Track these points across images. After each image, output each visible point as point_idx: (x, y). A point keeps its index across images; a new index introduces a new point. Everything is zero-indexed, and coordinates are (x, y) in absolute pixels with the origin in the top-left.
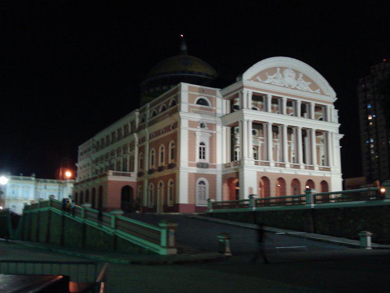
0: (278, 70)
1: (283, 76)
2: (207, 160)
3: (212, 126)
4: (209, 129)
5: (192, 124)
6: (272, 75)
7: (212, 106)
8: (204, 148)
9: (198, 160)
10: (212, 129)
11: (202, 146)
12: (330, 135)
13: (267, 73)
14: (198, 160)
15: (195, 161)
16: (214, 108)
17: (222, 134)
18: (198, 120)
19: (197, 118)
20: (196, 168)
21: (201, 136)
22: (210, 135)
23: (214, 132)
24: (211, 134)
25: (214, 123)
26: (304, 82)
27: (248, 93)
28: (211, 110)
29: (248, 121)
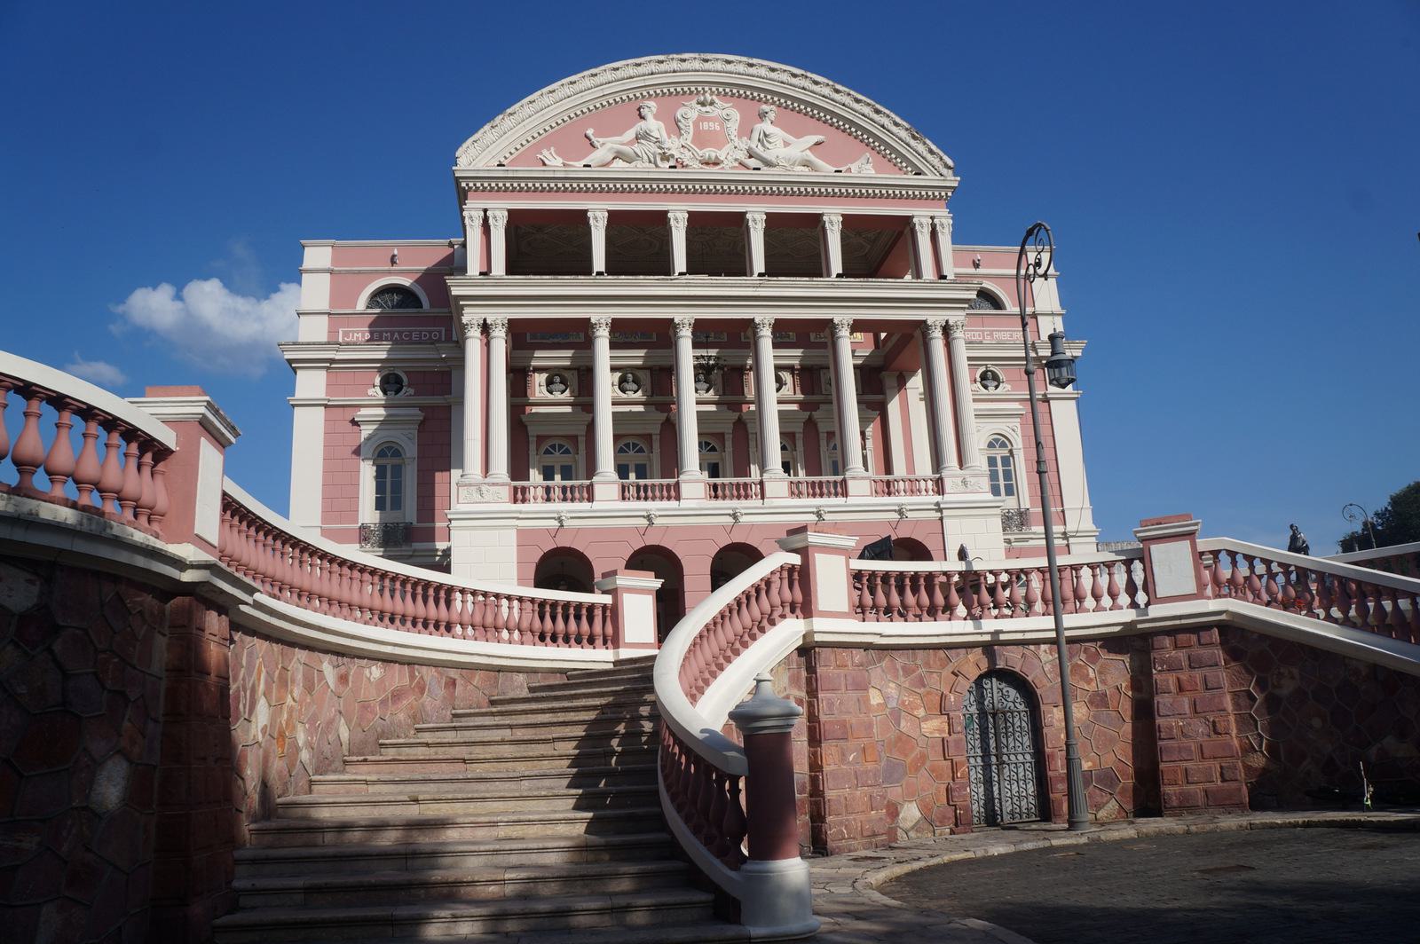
1: (676, 127)
6: (620, 135)
12: (937, 334)
13: (590, 132)
24: (422, 408)
26: (790, 138)
27: (486, 219)
29: (486, 328)
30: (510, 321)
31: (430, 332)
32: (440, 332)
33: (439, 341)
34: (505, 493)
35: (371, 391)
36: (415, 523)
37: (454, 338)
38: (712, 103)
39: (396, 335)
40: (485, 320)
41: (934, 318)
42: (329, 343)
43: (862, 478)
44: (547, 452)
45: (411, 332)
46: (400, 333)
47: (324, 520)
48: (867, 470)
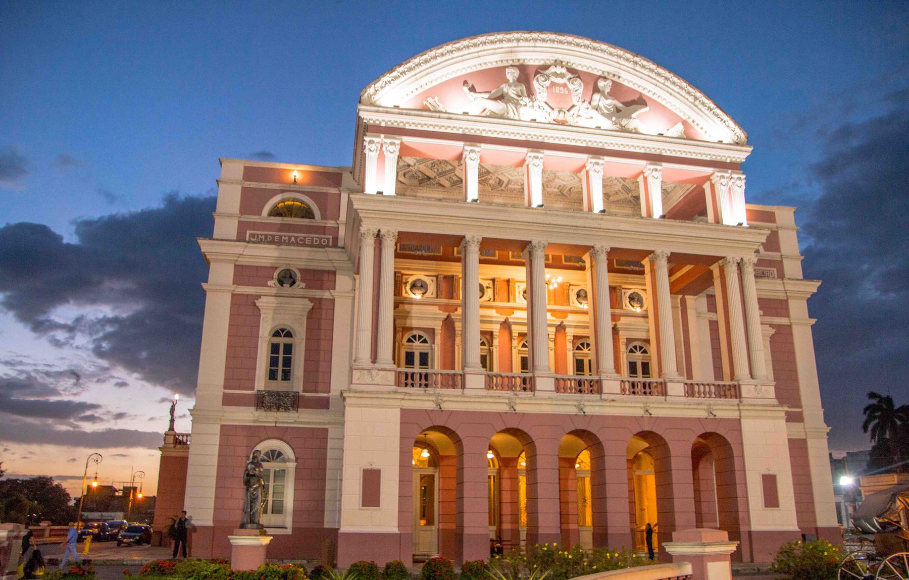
0: (512, 75)
2: (297, 384)
3: (320, 278)
4: (307, 287)
5: (244, 274)
7: (324, 217)
8: (288, 348)
9: (261, 383)
10: (321, 288)
11: (282, 341)
14: (261, 383)
15: (252, 388)
16: (331, 223)
17: (354, 298)
18: (267, 263)
19: (265, 255)
20: (252, 409)
21: (276, 310)
22: (310, 305)
23: (326, 295)
24: (311, 299)
25: (327, 266)
28: (323, 230)
30: (400, 234)
31: (320, 239)
32: (328, 240)
33: (327, 246)
34: (391, 376)
35: (270, 283)
36: (301, 393)
37: (341, 244)
38: (562, 76)
39: (293, 239)
40: (379, 231)
41: (733, 256)
42: (238, 240)
43: (678, 382)
44: (409, 341)
45: (305, 238)
46: (296, 238)
47: (225, 388)
48: (681, 374)
